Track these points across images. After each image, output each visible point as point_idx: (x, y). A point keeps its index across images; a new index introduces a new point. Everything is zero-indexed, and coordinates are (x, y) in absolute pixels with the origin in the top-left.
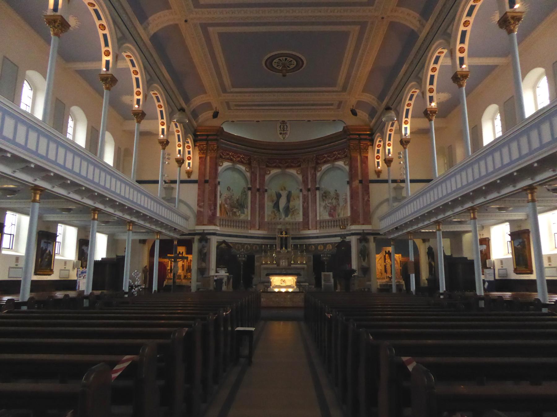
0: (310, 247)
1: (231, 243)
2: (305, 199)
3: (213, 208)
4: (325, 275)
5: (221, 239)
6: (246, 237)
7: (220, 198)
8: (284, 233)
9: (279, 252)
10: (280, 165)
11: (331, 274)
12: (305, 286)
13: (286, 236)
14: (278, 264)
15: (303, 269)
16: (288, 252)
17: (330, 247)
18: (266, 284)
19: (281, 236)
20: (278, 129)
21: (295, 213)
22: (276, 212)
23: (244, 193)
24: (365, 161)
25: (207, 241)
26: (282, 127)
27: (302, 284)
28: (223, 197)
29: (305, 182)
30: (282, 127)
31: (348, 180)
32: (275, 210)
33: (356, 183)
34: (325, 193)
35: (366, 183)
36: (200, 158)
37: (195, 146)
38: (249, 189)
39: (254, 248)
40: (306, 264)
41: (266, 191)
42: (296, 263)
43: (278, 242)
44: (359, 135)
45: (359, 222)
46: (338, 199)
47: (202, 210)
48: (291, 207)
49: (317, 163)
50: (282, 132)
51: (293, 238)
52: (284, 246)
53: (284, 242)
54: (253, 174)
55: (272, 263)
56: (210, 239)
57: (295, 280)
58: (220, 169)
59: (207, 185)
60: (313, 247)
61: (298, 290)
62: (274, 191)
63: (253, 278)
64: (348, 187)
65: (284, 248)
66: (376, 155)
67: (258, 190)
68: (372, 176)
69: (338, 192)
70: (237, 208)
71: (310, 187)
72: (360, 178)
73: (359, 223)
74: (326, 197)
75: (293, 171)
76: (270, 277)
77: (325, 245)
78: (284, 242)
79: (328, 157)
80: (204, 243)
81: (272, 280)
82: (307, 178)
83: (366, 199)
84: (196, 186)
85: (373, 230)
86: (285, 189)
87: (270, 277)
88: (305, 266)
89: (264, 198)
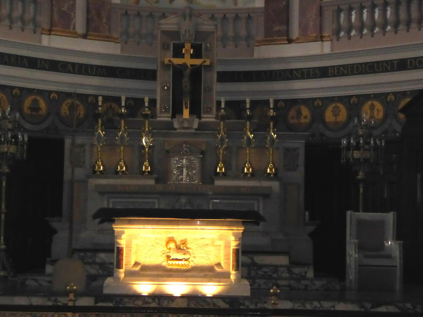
0: (292, 112)
4: (360, 223)
6: (33, 63)
8: (187, 50)
9: (169, 126)
11: (390, 218)
12: (276, 268)
13: (197, 62)
14: (161, 175)
16: (202, 127)
17: (372, 113)
18: (102, 256)
19: (177, 61)
27: (260, 259)
39: (65, 109)
40: (276, 176)
43: (159, 90)
51: (225, 77)
52: (187, 101)
53: (186, 83)
55: (135, 171)
57: (233, 244)
60: (305, 111)
63: (55, 232)
65: (186, 113)
76: (117, 228)
77: (354, 104)
81: (123, 242)
87: (117, 228)
88: (275, 185)
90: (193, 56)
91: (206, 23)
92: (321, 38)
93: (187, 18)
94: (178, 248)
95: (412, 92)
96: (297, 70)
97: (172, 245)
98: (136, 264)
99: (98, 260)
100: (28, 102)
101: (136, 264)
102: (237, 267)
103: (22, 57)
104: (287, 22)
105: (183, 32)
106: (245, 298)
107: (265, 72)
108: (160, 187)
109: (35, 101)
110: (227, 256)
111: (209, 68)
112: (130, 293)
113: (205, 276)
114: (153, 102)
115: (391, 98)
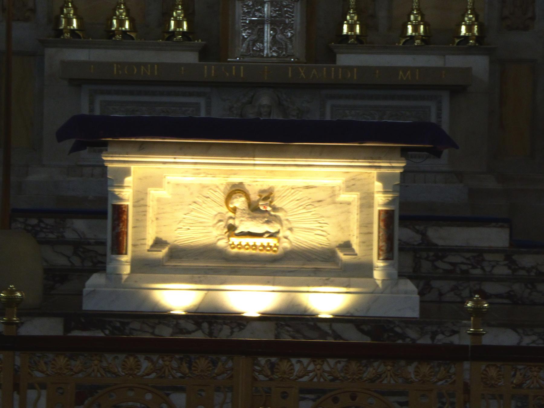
12: (478, 254)
15: (458, 88)
40: (480, 44)
42: (381, 33)
57: (380, 200)
61: (407, 303)
76: (113, 161)
81: (127, 194)
87: (113, 161)
88: (479, 64)
94: (254, 209)
97: (239, 202)
98: (159, 243)
99: (69, 235)
101: (159, 243)
102: (388, 253)
106: (408, 322)
108: (210, 70)
110: (365, 225)
112: (144, 309)
113: (316, 272)
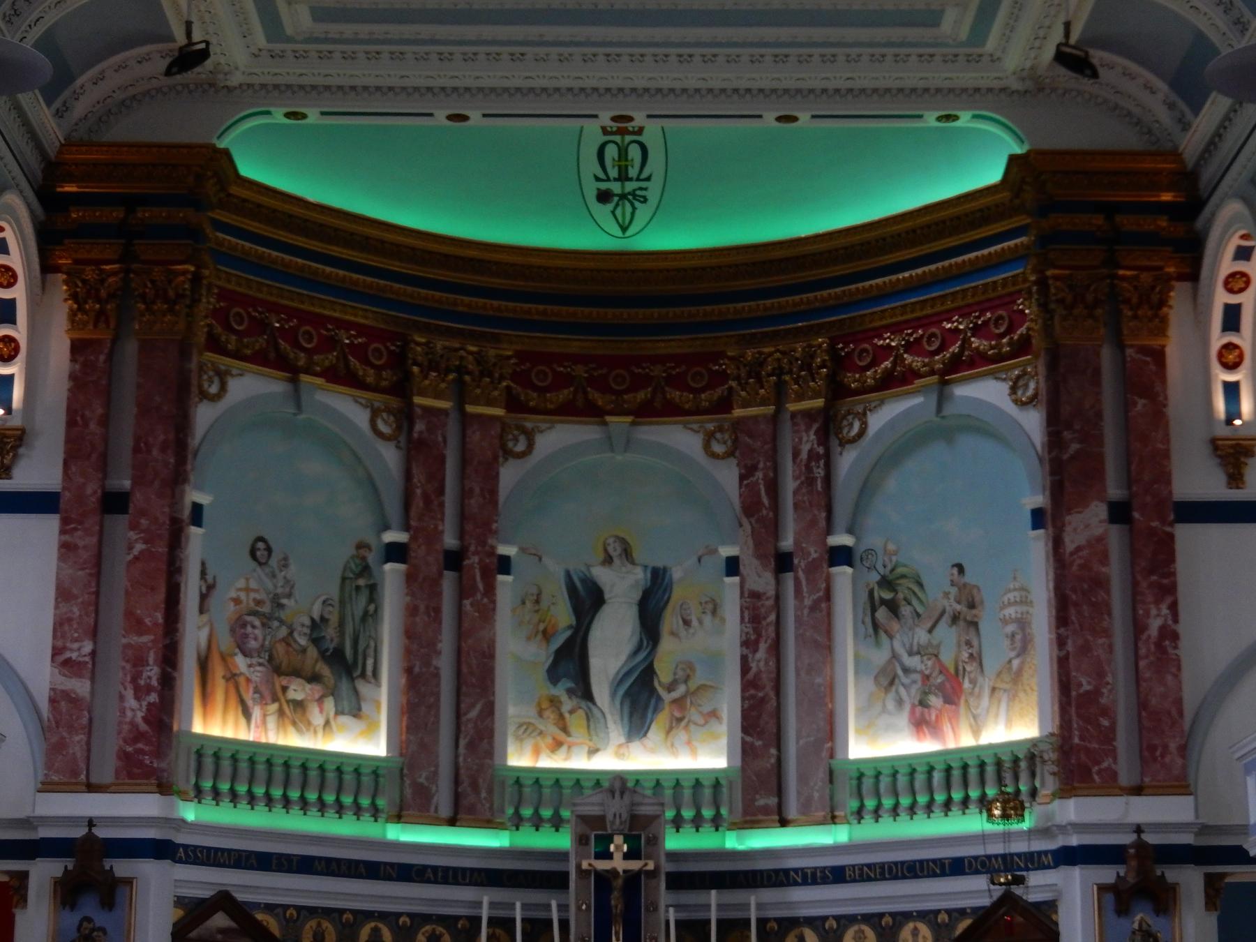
1: (270, 908)
2: (761, 622)
3: (152, 673)
5: (202, 881)
7: (201, 611)
8: (619, 845)
10: (600, 399)
13: (634, 865)
19: (602, 865)
20: (590, 166)
21: (693, 714)
22: (567, 704)
23: (360, 579)
24: (1146, 380)
25: (112, 892)
26: (611, 152)
28: (224, 610)
29: (760, 510)
30: (611, 152)
31: (1039, 500)
32: (560, 691)
33: (1090, 521)
34: (886, 583)
35: (1152, 524)
36: (77, 348)
37: (47, 268)
38: (395, 553)
41: (504, 565)
44: (1109, 210)
45: (1114, 775)
46: (974, 625)
47: (81, 687)
48: (664, 672)
49: (837, 391)
50: (616, 187)
51: (679, 881)
53: (616, 901)
54: (419, 452)
56: (129, 882)
58: (204, 415)
59: (119, 525)
62: (555, 569)
64: (1036, 546)
66: (1218, 339)
67: (454, 560)
68: (1197, 479)
69: (969, 578)
70: (314, 678)
71: (787, 543)
72: (1115, 491)
73: (1110, 786)
74: (893, 607)
75: (682, 438)
78: (616, 901)
79: (909, 347)
80: (89, 907)
82: (774, 487)
83: (1155, 625)
84: (46, 528)
85: (1204, 829)
86: (627, 553)
89: (488, 613)
90: (627, 856)
91: (646, 801)
92: (833, 819)
93: (617, 795)
95: (975, 910)
96: (796, 870)
100: (365, 933)
103: (358, 862)
104: (780, 791)
105: (610, 817)
107: (746, 873)
109: (376, 930)
111: (653, 874)
114: (564, 925)
115: (943, 917)
